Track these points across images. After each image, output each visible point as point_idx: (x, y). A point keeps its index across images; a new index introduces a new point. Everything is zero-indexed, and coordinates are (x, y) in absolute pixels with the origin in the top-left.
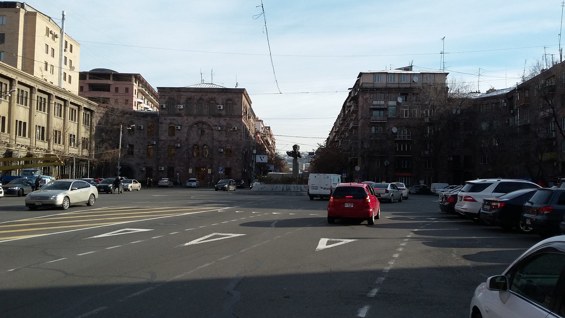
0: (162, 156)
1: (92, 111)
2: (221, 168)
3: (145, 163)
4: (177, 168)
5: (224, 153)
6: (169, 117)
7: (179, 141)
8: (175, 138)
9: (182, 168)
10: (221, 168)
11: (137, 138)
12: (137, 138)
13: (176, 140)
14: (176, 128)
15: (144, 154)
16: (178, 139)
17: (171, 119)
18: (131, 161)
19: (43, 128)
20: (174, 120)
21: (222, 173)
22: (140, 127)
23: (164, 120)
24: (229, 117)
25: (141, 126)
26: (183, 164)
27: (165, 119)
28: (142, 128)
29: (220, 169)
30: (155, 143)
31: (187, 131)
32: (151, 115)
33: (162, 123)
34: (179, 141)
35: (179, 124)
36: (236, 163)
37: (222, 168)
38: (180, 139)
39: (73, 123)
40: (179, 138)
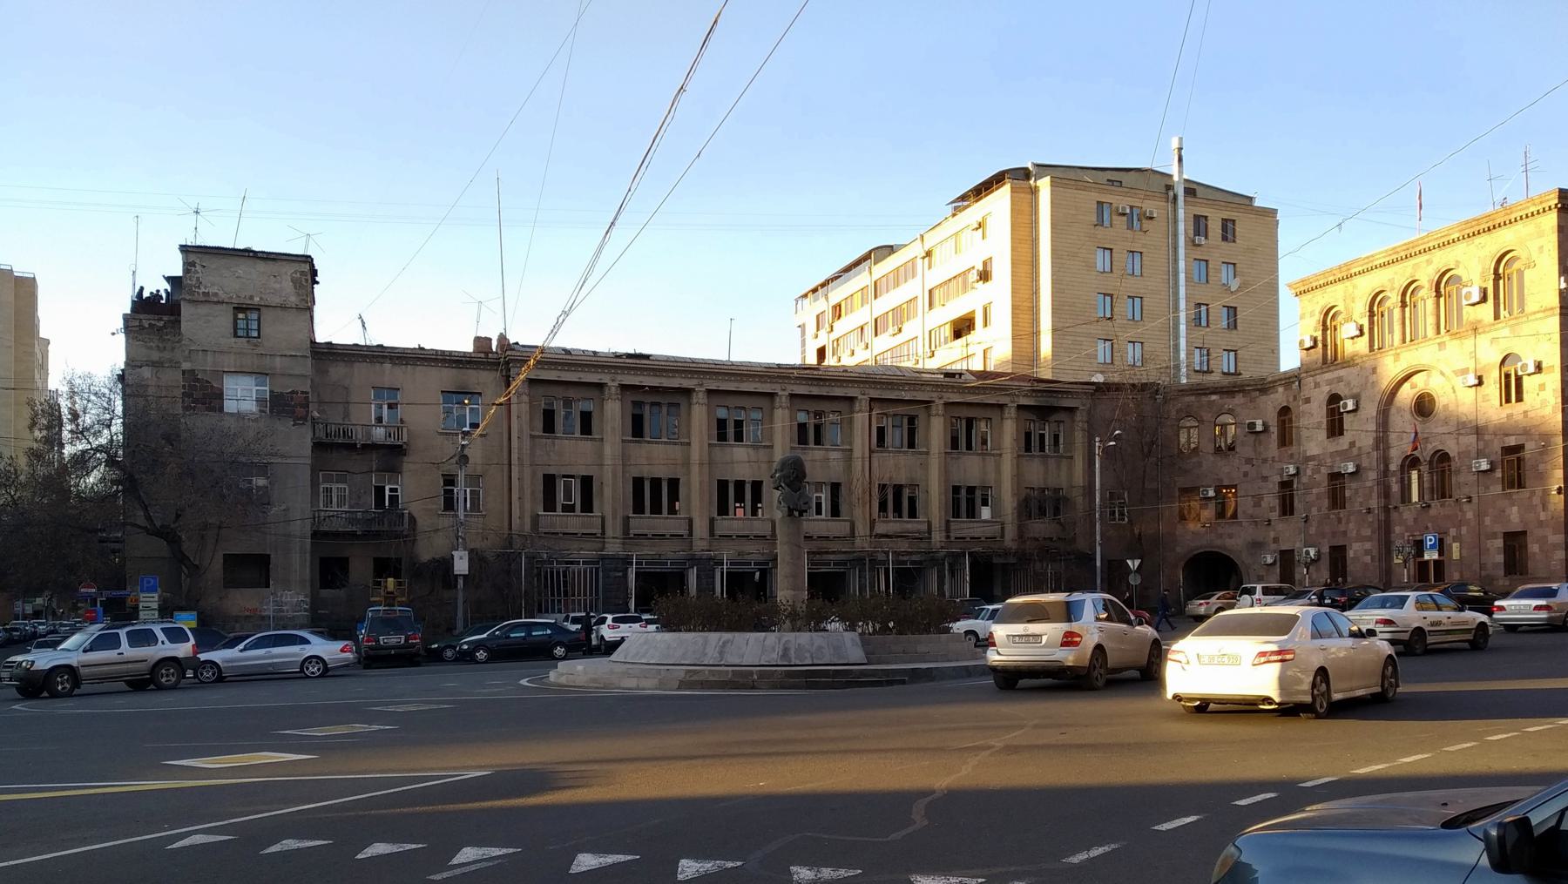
0: (1314, 511)
1: (1071, 410)
2: (1431, 540)
3: (1276, 540)
4: (1355, 550)
5: (1498, 474)
6: (1328, 376)
7: (1355, 451)
8: (1343, 442)
9: (1368, 545)
10: (1431, 540)
11: (1249, 461)
12: (1249, 461)
13: (1347, 450)
14: (1342, 410)
15: (1272, 509)
16: (1352, 444)
17: (1330, 382)
18: (1231, 536)
19: (835, 488)
20: (1339, 382)
21: (1436, 556)
22: (1252, 425)
23: (1315, 388)
24: (1511, 326)
25: (1254, 424)
26: (1369, 534)
27: (1317, 385)
28: (1259, 428)
29: (1429, 543)
30: (1292, 470)
31: (1375, 414)
32: (1280, 380)
33: (1308, 401)
34: (1355, 451)
35: (1355, 391)
36: (1543, 511)
37: (1434, 536)
38: (1357, 445)
39: (978, 454)
40: (1354, 442)
